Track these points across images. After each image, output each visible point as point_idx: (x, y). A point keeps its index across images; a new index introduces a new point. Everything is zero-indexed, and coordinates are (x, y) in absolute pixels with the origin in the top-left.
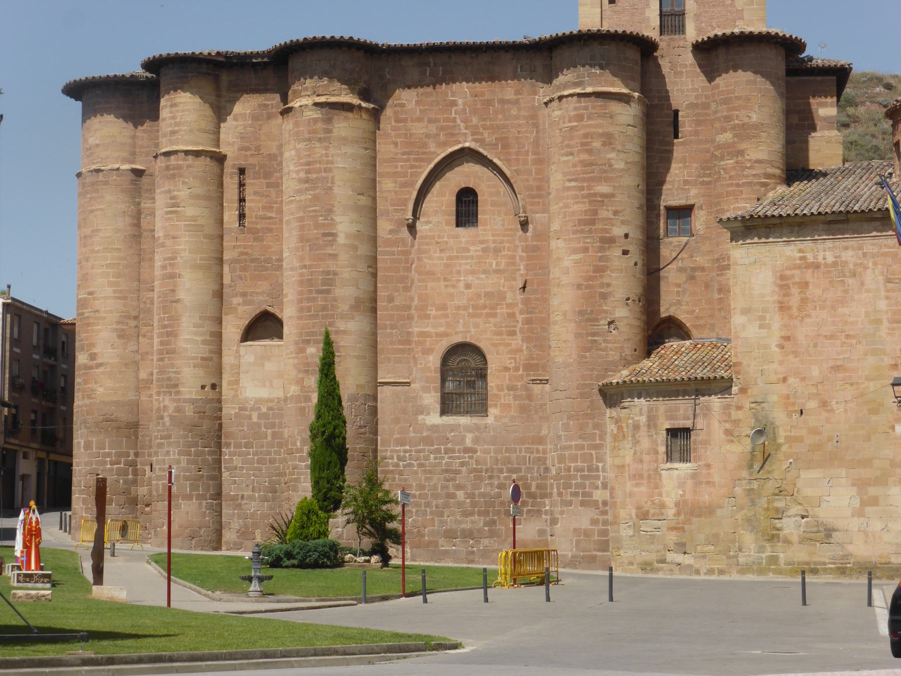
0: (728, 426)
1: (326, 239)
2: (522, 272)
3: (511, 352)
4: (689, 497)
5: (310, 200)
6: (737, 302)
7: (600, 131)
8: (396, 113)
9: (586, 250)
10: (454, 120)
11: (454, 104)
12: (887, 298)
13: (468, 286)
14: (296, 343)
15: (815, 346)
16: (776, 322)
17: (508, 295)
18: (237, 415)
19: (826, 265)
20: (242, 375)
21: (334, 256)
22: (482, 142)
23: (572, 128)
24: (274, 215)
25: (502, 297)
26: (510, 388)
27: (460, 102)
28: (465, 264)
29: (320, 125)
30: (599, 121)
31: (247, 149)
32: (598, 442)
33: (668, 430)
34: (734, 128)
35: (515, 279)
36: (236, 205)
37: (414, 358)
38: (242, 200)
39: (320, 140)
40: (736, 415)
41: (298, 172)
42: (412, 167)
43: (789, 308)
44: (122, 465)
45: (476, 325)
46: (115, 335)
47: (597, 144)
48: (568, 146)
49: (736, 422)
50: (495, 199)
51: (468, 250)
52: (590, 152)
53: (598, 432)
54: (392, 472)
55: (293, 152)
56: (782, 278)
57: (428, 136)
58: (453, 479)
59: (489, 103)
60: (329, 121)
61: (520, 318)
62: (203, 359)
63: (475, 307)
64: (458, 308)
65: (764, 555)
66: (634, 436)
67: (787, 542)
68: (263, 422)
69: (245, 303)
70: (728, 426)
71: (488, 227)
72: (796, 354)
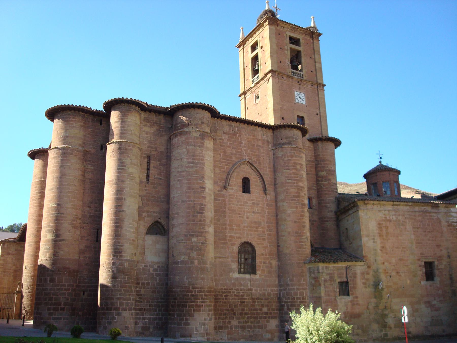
0: (364, 281)
1: (202, 189)
2: (267, 214)
3: (264, 247)
4: (349, 310)
5: (194, 171)
6: (364, 233)
7: (299, 162)
8: (220, 142)
9: (297, 207)
10: (241, 149)
11: (241, 143)
12: (414, 234)
13: (248, 218)
14: (186, 236)
15: (393, 250)
16: (378, 240)
17: (262, 223)
18: (143, 269)
19: (393, 221)
20: (146, 250)
21: (204, 197)
22: (251, 159)
23: (289, 160)
24: (162, 178)
25: (260, 223)
26: (265, 263)
27: (243, 142)
28: (247, 208)
29: (199, 140)
30: (299, 159)
31: (151, 148)
32: (305, 287)
33: (339, 282)
34: (326, 170)
35: (264, 217)
36: (146, 171)
37: (228, 247)
38: (148, 169)
39: (199, 146)
40: (366, 276)
41: (188, 159)
42: (226, 165)
43: (383, 236)
44: (70, 291)
45: (251, 235)
46: (71, 226)
47: (298, 167)
48: (287, 166)
49: (367, 280)
50: (256, 183)
51: (247, 203)
52: (296, 169)
53: (305, 282)
54: (219, 299)
55: (185, 150)
56: (379, 224)
57: (232, 154)
58: (244, 302)
59: (254, 145)
60: (203, 139)
61: (267, 233)
62: (133, 240)
63: (251, 227)
64: (244, 227)
65: (382, 333)
66: (324, 285)
67: (390, 328)
68: (155, 273)
69: (148, 216)
70: (364, 281)
71: (254, 194)
72: (387, 253)
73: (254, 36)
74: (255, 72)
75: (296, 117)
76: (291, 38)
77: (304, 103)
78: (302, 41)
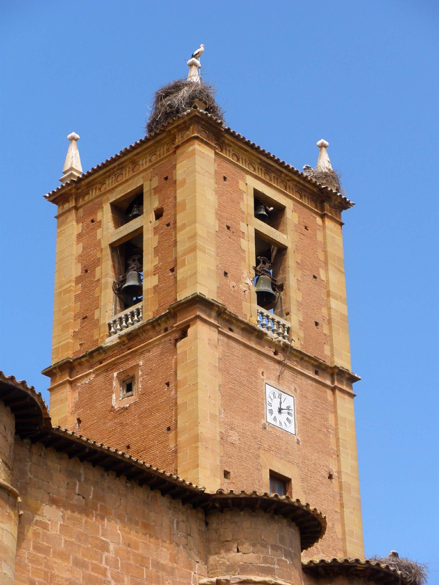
10: (104, 572)
11: (105, 547)
27: (112, 547)
73: (127, 174)
74: (128, 295)
75: (267, 476)
76: (260, 200)
77: (291, 429)
78: (291, 215)
